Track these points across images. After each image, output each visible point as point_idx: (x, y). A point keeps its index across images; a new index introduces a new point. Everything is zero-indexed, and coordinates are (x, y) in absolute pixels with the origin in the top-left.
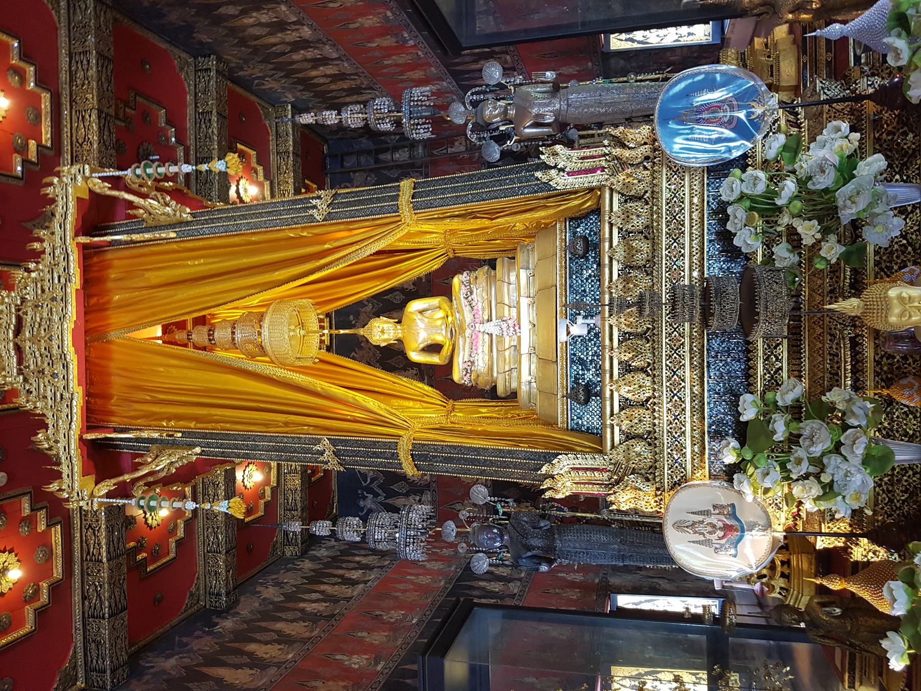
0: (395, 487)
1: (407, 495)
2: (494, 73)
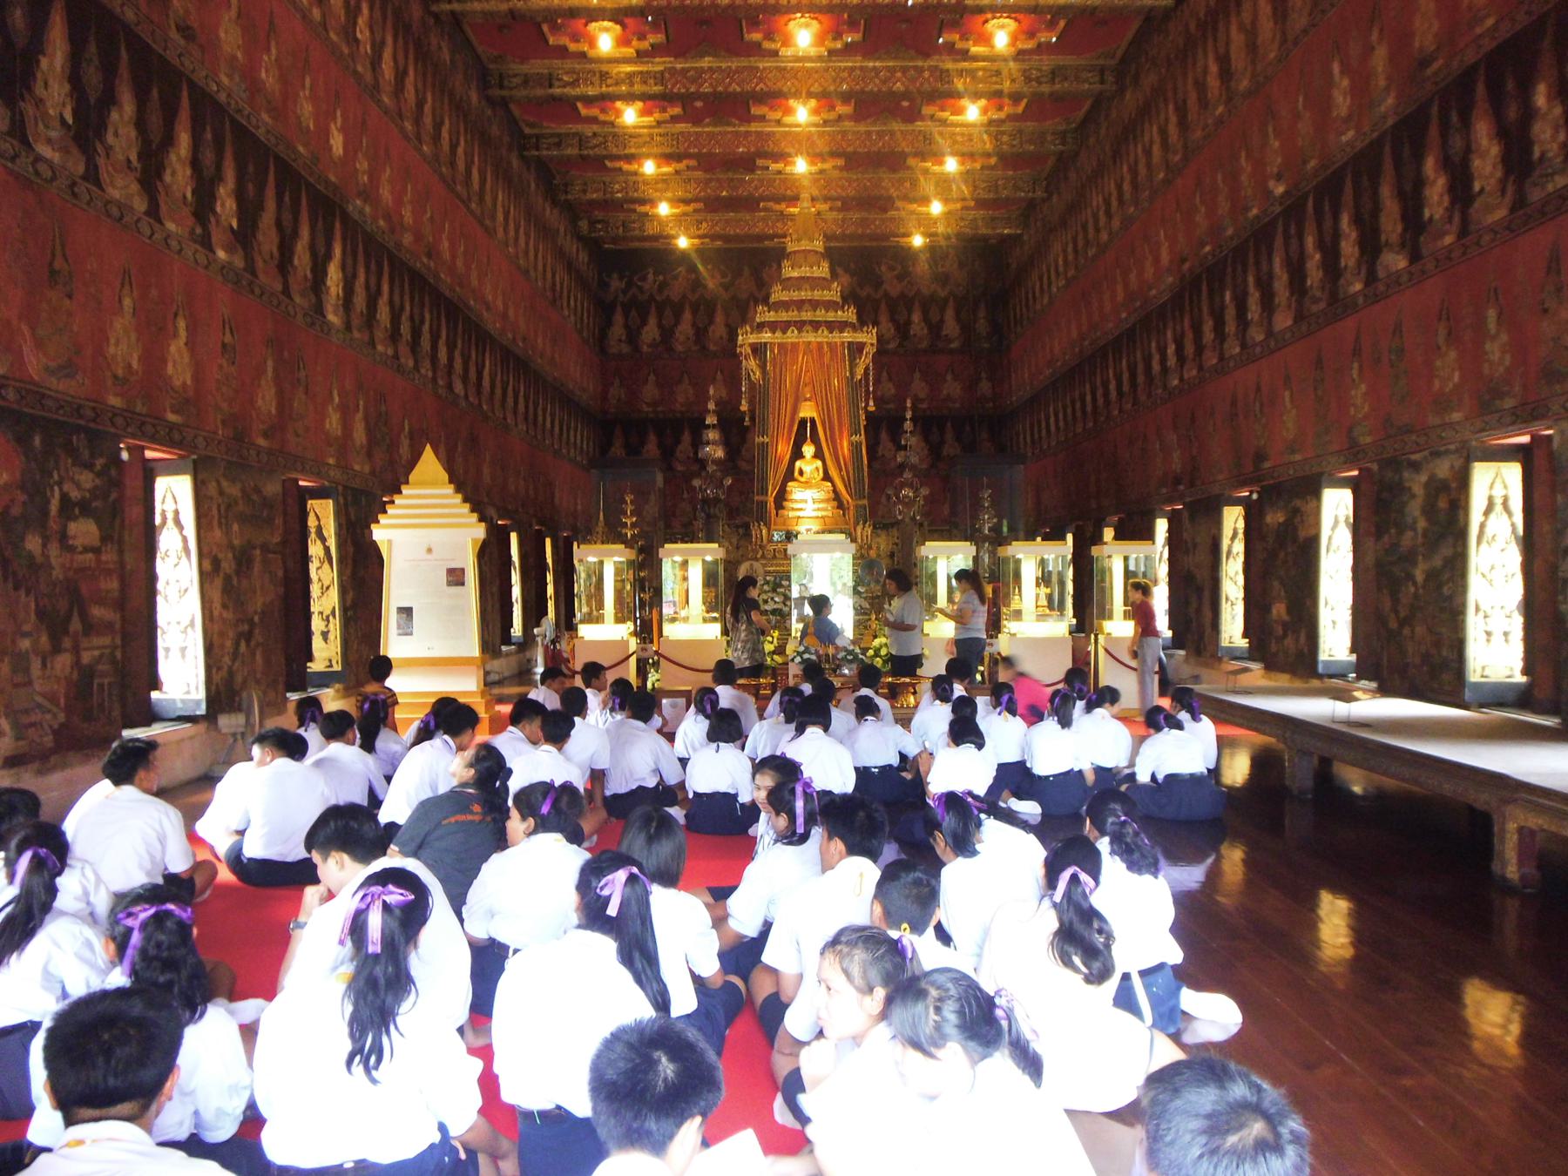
0: (633, 313)
1: (626, 326)
2: (924, 491)
